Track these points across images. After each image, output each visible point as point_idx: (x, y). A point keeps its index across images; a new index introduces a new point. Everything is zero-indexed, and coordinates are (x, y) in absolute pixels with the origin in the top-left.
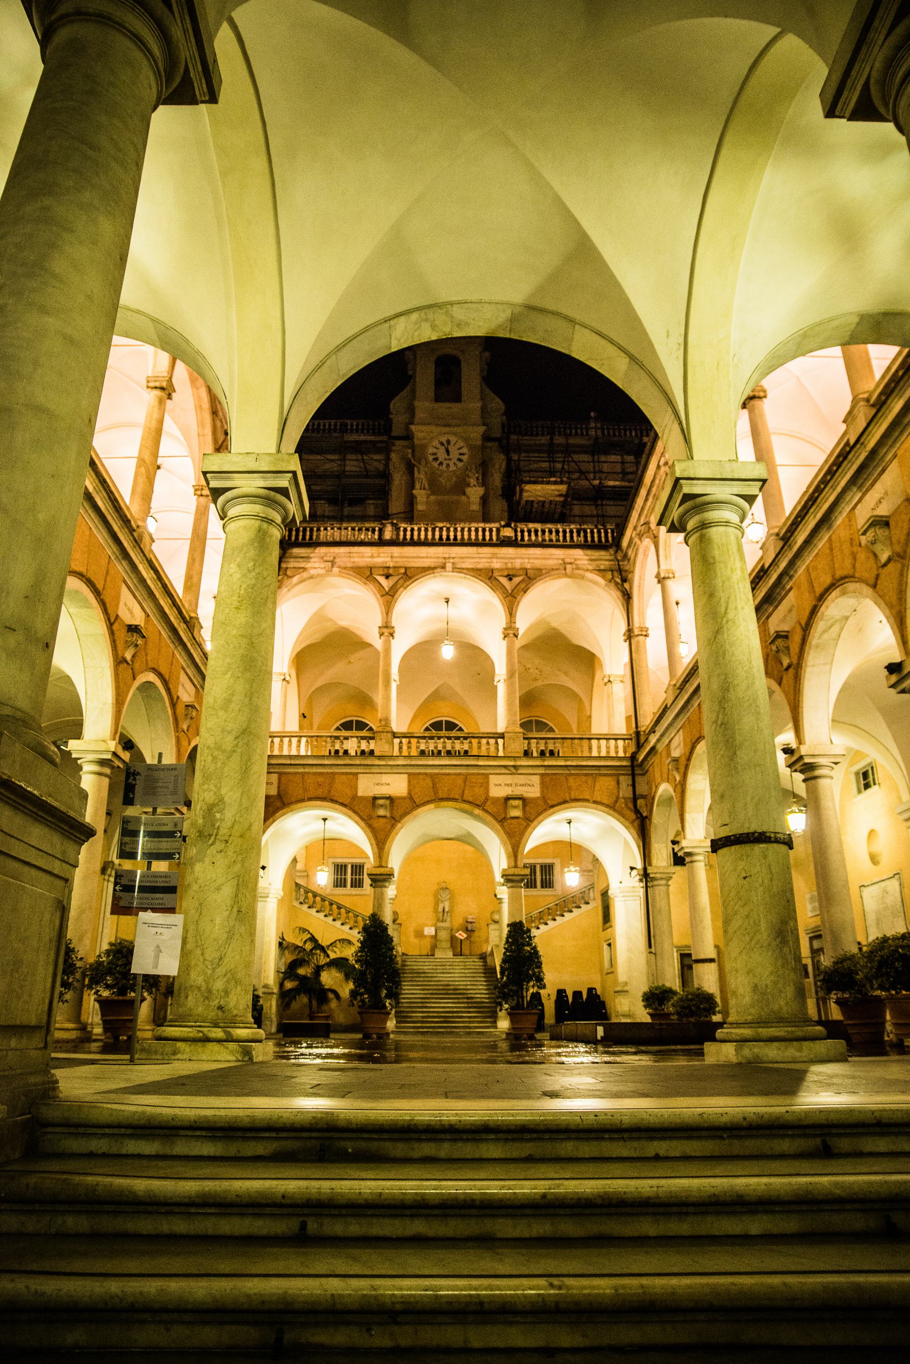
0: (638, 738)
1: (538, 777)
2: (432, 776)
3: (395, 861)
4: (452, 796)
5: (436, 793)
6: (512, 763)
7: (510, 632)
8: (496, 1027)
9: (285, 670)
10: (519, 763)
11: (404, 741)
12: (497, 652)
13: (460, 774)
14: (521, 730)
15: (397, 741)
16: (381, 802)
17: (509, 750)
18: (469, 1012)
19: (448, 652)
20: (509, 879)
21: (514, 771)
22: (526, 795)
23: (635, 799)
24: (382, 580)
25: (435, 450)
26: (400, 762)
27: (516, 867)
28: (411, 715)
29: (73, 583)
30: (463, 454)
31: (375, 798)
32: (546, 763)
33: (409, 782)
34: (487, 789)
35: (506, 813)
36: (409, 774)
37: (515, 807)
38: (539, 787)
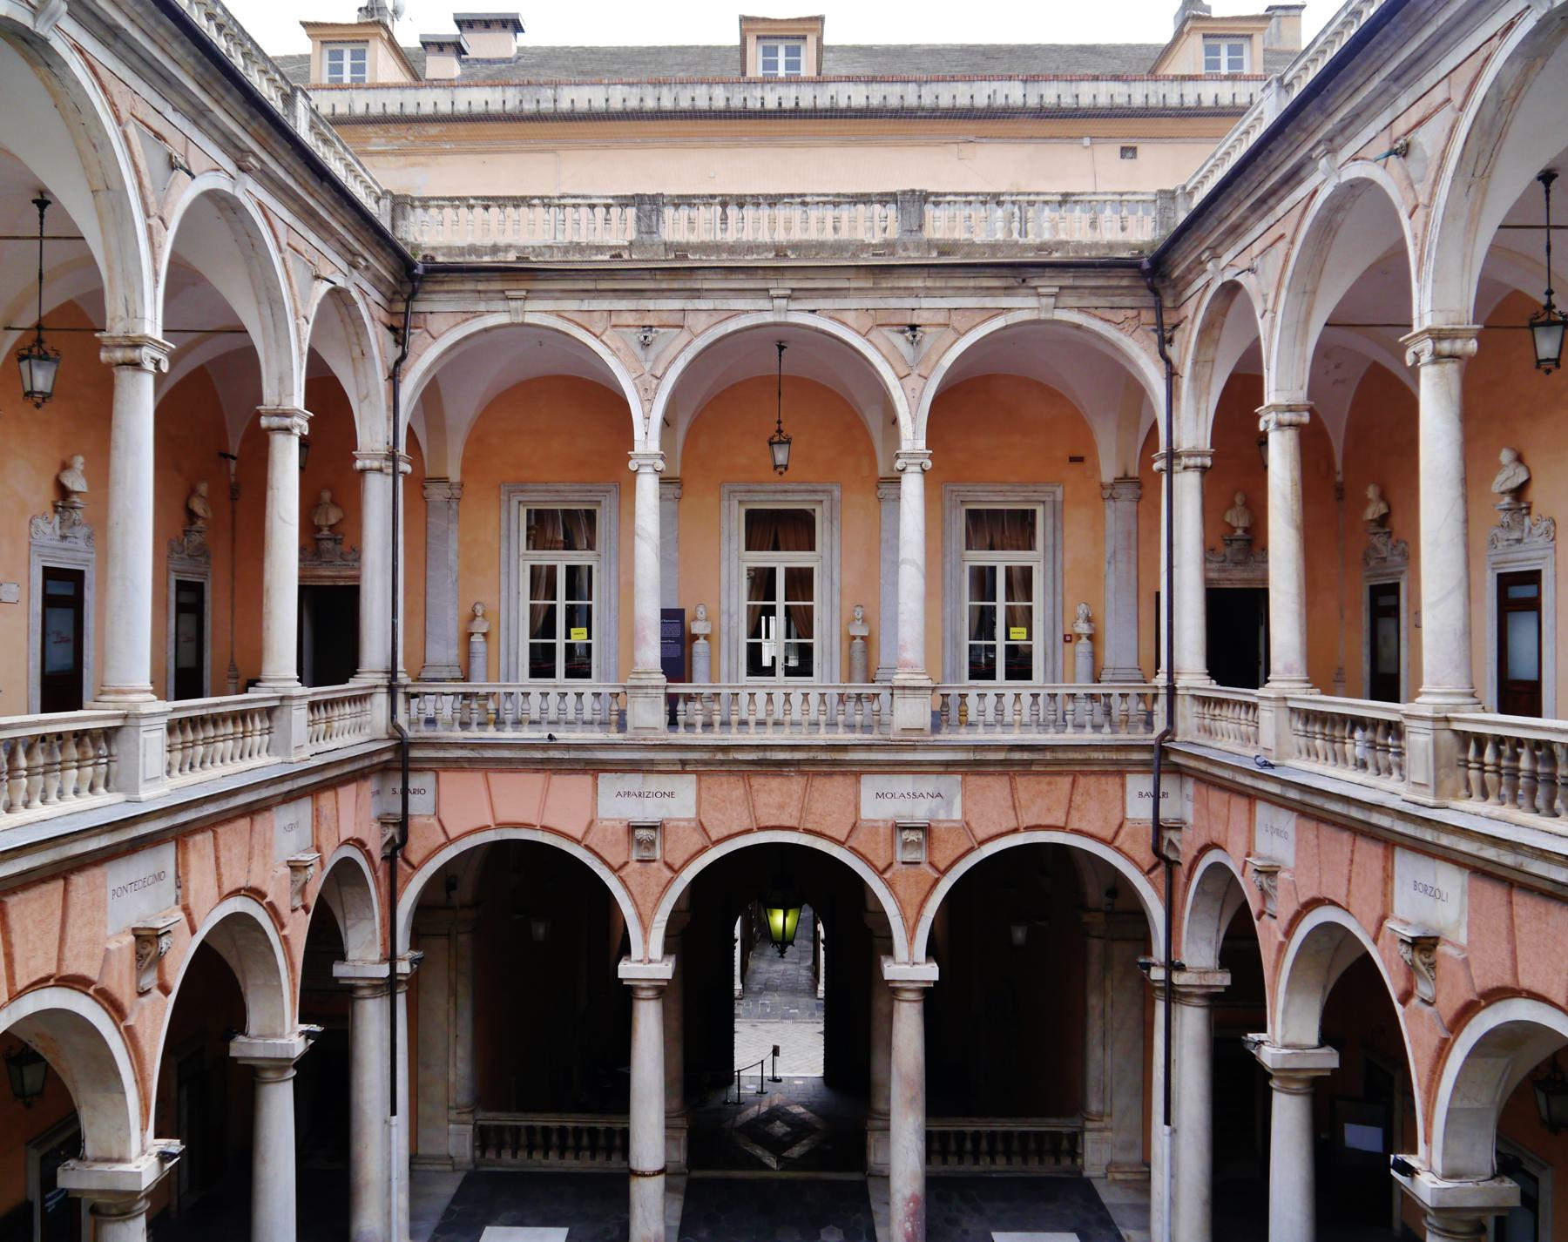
31: (632, 828)
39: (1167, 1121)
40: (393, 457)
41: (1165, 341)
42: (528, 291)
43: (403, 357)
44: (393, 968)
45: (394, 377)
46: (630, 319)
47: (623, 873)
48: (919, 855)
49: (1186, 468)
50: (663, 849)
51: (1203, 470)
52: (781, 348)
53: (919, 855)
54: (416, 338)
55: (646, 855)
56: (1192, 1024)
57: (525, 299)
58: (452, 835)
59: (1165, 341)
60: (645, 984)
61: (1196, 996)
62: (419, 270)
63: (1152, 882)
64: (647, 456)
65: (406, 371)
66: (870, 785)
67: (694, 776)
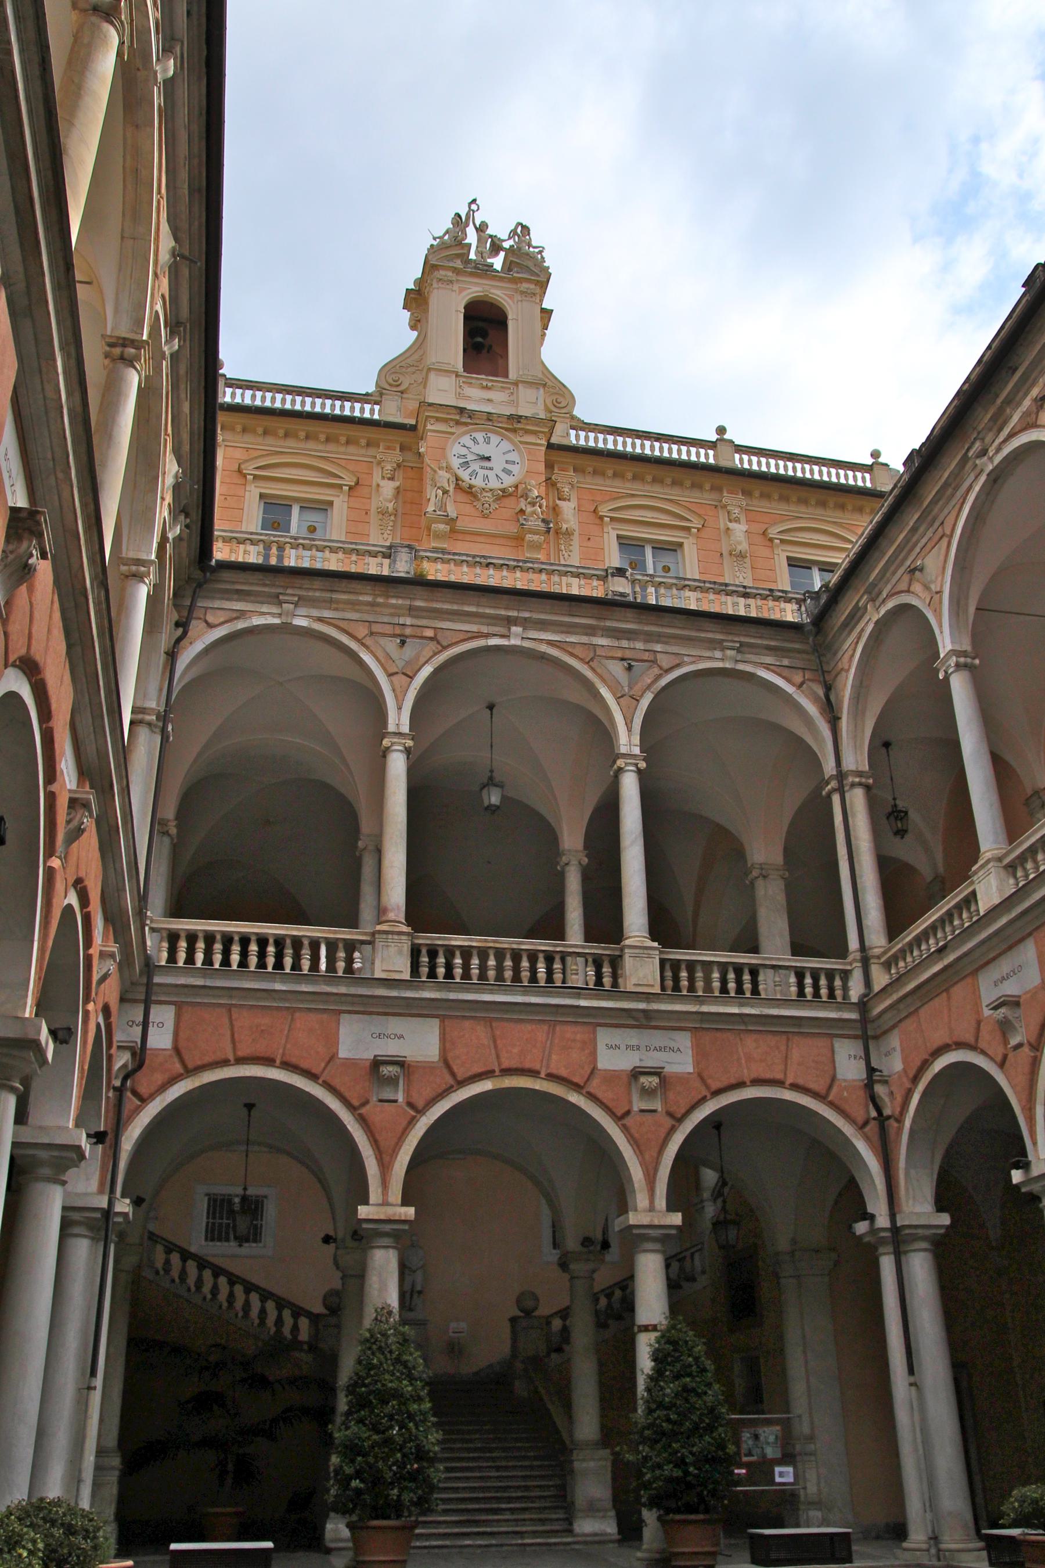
1: (688, 1034)
4: (527, 1065)
6: (642, 1006)
8: (570, 1531)
10: (655, 1006)
14: (656, 944)
16: (387, 1070)
17: (634, 981)
18: (510, 1500)
21: (644, 1022)
22: (669, 1069)
24: (391, 645)
25: (464, 451)
30: (513, 463)
31: (377, 1063)
32: (705, 1009)
34: (594, 1054)
38: (690, 1052)
39: (911, 1371)
40: (164, 718)
41: (828, 688)
42: (300, 598)
43: (185, 634)
44: (111, 1203)
45: (172, 656)
46: (388, 629)
47: (363, 1111)
48: (657, 1105)
49: (853, 785)
50: (407, 1092)
51: (868, 788)
52: (491, 707)
53: (657, 1105)
54: (196, 626)
55: (388, 1094)
56: (920, 1267)
57: (296, 605)
58: (190, 1066)
59: (828, 688)
60: (387, 1228)
61: (924, 1238)
62: (213, 563)
63: (867, 1139)
64: (400, 734)
65: (185, 648)
66: (604, 1037)
67: (436, 1023)
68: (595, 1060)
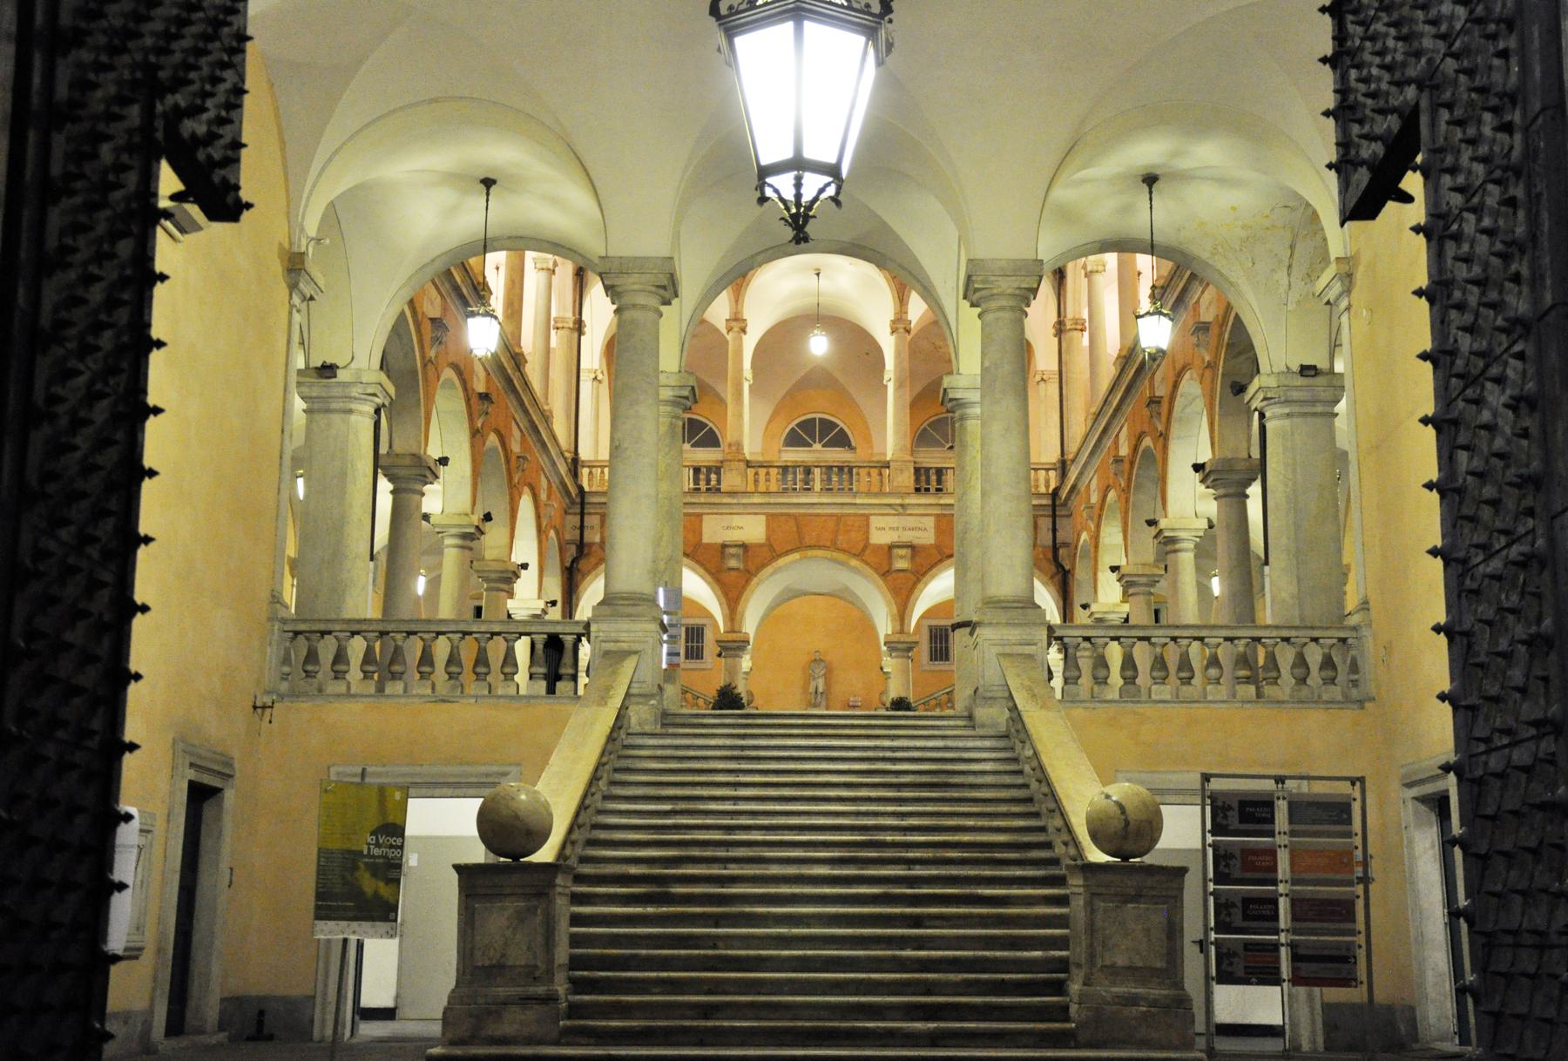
0: (1063, 467)
2: (795, 517)
3: (750, 626)
5: (801, 539)
6: (899, 501)
7: (899, 324)
9: (596, 366)
10: (907, 501)
11: (762, 472)
12: (888, 345)
13: (832, 515)
15: (751, 472)
16: (732, 551)
19: (819, 345)
20: (892, 646)
22: (916, 542)
23: (1055, 549)
26: (757, 499)
27: (902, 632)
28: (770, 412)
29: (449, 373)
31: (724, 546)
32: (942, 502)
33: (768, 526)
34: (867, 532)
35: (890, 564)
36: (767, 515)
37: (902, 557)
68: (868, 538)
